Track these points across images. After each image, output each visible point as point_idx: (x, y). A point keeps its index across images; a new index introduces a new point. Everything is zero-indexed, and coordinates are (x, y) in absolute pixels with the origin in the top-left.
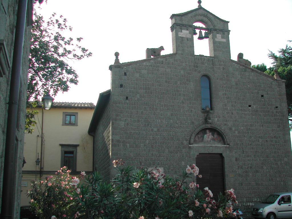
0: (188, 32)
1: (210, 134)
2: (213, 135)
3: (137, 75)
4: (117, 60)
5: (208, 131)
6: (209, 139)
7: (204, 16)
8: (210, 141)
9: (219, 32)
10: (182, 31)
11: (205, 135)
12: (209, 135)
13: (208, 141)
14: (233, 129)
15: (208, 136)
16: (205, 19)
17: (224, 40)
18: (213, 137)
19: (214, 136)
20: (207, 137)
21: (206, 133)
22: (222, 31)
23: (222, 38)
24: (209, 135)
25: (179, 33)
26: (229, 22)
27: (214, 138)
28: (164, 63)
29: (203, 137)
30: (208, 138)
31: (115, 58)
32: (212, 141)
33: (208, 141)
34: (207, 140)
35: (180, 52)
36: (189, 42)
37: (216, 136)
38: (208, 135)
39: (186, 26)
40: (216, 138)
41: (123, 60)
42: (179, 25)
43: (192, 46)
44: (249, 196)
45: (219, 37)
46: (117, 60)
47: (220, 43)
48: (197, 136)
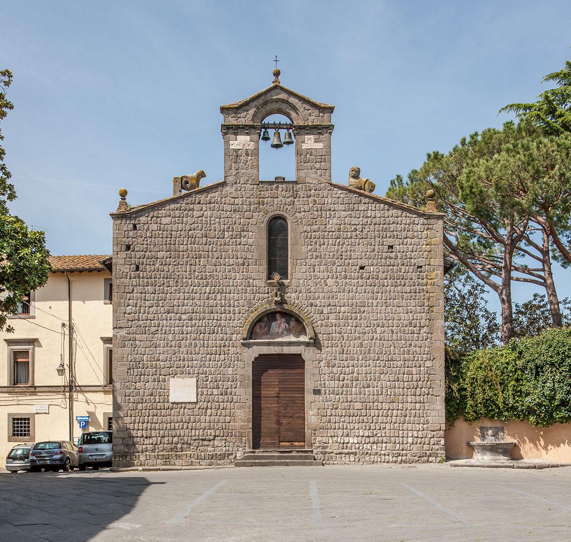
0: (248, 138)
1: (283, 320)
3: (155, 227)
5: (278, 315)
6: (280, 330)
7: (283, 102)
8: (282, 333)
9: (311, 129)
10: (236, 138)
11: (273, 323)
12: (281, 323)
13: (278, 333)
14: (325, 310)
15: (279, 325)
16: (284, 106)
17: (320, 146)
18: (287, 326)
19: (289, 324)
20: (277, 326)
21: (275, 320)
22: (317, 128)
24: (281, 323)
25: (231, 142)
27: (289, 327)
28: (201, 202)
29: (270, 327)
30: (279, 328)
31: (119, 198)
32: (285, 332)
33: (278, 333)
34: (277, 331)
35: (231, 179)
36: (249, 158)
37: (293, 323)
38: (279, 322)
39: (243, 128)
40: (294, 327)
42: (232, 128)
44: (349, 428)
45: (310, 142)
47: (310, 152)
48: (258, 326)
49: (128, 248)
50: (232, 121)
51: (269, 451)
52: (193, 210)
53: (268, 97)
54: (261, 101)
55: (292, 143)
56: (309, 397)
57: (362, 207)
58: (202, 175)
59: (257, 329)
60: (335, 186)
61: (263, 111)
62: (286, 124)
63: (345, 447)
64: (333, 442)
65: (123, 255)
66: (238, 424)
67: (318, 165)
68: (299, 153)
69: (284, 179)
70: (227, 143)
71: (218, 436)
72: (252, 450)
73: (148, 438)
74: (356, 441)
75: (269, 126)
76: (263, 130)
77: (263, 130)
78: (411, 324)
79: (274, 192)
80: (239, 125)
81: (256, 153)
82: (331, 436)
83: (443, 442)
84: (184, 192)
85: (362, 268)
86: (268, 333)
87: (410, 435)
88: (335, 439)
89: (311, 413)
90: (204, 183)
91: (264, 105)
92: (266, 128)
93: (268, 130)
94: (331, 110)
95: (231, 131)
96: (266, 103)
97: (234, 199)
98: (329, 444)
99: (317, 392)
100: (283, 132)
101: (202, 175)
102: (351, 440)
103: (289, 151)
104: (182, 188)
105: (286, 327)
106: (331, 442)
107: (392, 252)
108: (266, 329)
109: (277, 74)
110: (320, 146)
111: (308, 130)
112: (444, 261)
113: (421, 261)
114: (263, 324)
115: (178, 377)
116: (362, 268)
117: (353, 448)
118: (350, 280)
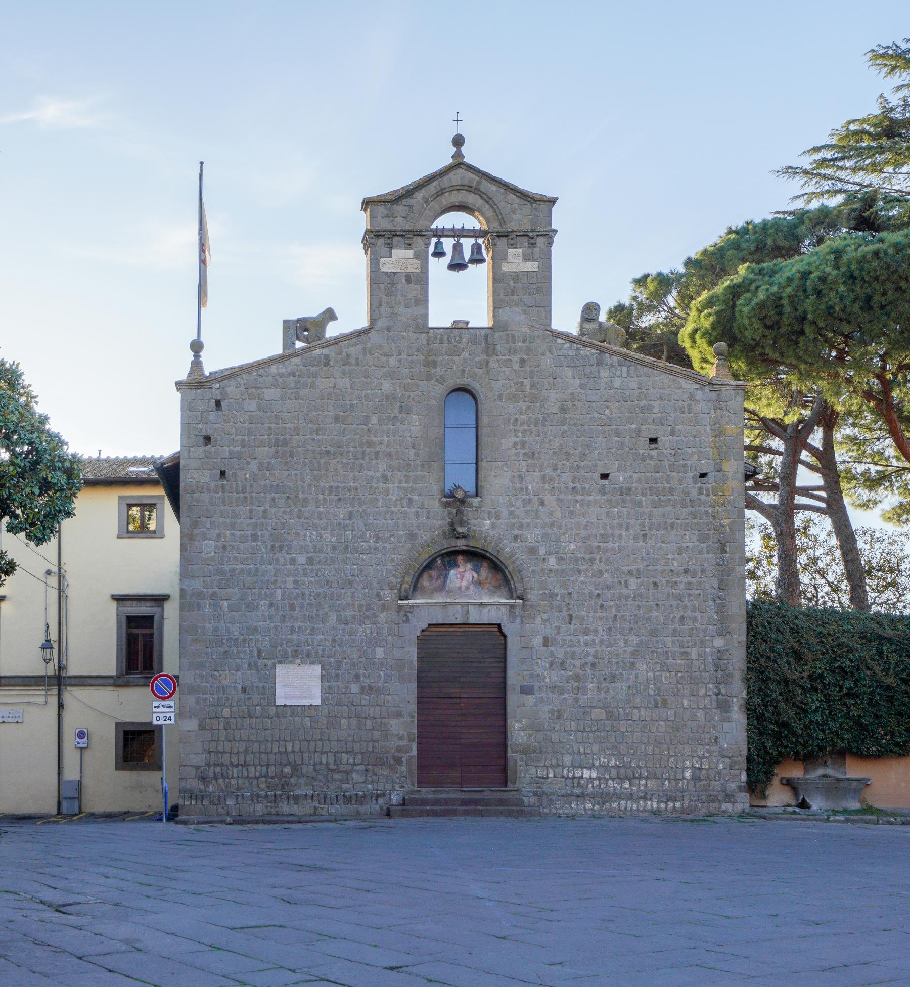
1: (469, 566)
2: (476, 570)
3: (252, 405)
4: (197, 364)
6: (464, 583)
8: (467, 588)
10: (391, 254)
13: (460, 588)
14: (542, 550)
16: (471, 199)
17: (532, 267)
18: (476, 575)
19: (478, 573)
20: (459, 576)
21: (456, 565)
23: (527, 259)
24: (465, 571)
25: (382, 260)
26: (552, 201)
28: (331, 363)
29: (446, 577)
31: (190, 356)
32: (472, 587)
33: (460, 588)
36: (412, 286)
37: (485, 572)
38: (461, 569)
39: (402, 235)
40: (486, 579)
41: (211, 364)
43: (422, 301)
44: (582, 751)
46: (197, 364)
48: (425, 576)
49: (207, 439)
50: (385, 224)
51: (445, 791)
52: (315, 375)
53: (446, 181)
54: (433, 188)
55: (482, 261)
56: (513, 699)
57: (604, 373)
58: (329, 315)
59: (425, 582)
60: (558, 335)
61: (435, 205)
62: (474, 230)
63: (576, 785)
64: (555, 776)
65: (200, 451)
66: (394, 743)
67: (527, 299)
68: (498, 278)
69: (467, 323)
70: (374, 263)
71: (359, 764)
72: (415, 788)
73: (240, 767)
74: (594, 775)
75: (446, 233)
76: (434, 240)
77: (434, 240)
78: (686, 571)
79: (454, 346)
80: (395, 231)
81: (421, 279)
82: (552, 766)
83: (744, 777)
84: (299, 345)
85: (605, 476)
86: (442, 588)
87: (688, 764)
88: (558, 770)
89: (517, 726)
90: (332, 330)
91: (438, 196)
92: (439, 236)
93: (443, 240)
94: (552, 201)
95: (381, 241)
96: (440, 193)
97: (386, 358)
98: (549, 780)
99: (526, 690)
100: (467, 244)
101: (329, 315)
102: (586, 774)
103: (480, 274)
104: (298, 339)
105: (473, 577)
106: (551, 775)
107: (656, 448)
108: (439, 582)
109: (458, 141)
110: (532, 267)
111: (512, 239)
112: (746, 467)
113: (706, 465)
114: (434, 573)
115: (291, 662)
116: (605, 476)
117: (590, 786)
118: (583, 497)
